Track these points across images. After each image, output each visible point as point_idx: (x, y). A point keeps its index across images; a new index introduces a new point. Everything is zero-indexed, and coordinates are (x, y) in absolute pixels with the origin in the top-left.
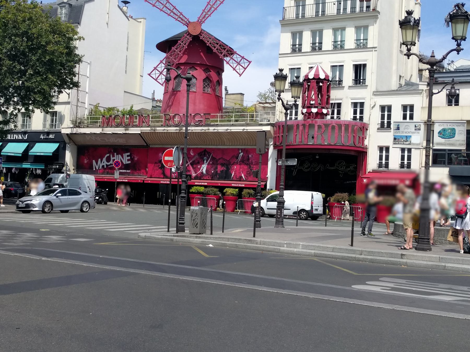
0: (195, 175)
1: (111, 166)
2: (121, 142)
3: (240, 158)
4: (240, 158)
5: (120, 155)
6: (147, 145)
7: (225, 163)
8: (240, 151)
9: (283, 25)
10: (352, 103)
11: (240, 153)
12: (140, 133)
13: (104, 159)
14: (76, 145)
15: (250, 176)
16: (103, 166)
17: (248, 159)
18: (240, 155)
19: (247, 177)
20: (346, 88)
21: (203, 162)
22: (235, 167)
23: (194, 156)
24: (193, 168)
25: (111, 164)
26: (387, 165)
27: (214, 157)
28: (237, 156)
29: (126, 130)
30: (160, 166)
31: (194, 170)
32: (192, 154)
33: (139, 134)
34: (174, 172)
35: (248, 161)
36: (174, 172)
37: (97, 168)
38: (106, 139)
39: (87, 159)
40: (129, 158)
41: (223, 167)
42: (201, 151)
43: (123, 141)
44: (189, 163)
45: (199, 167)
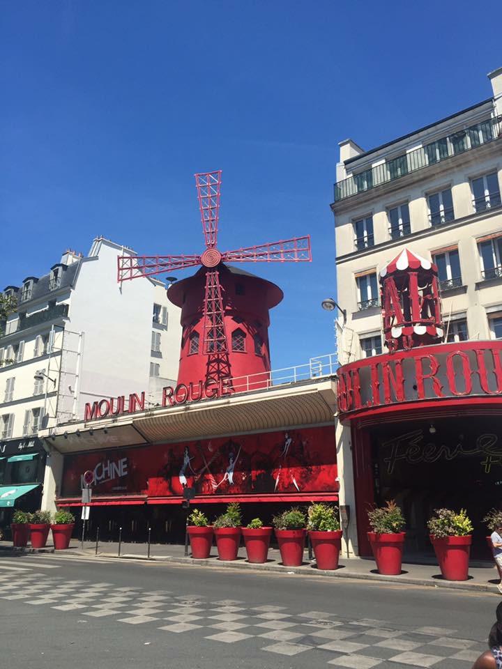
1: (103, 482)
2: (113, 440)
3: (286, 449)
5: (114, 464)
6: (148, 442)
8: (287, 437)
9: (336, 213)
10: (487, 314)
11: (286, 440)
12: (131, 422)
14: (62, 454)
19: (302, 483)
20: (471, 288)
25: (103, 479)
29: (114, 421)
32: (211, 450)
38: (92, 439)
40: (126, 466)
44: (207, 466)
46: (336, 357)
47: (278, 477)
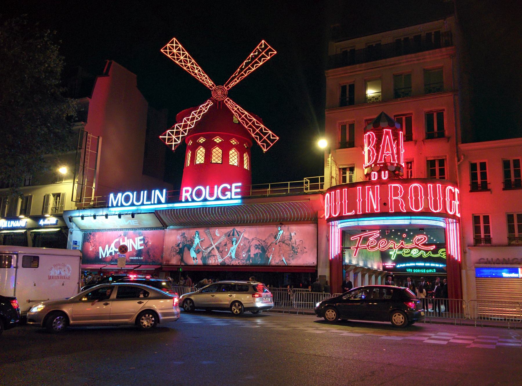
0: (221, 260)
4: (279, 238)
5: (131, 240)
7: (259, 245)
8: (279, 229)
13: (113, 245)
14: (82, 230)
15: (293, 259)
16: (111, 254)
17: (291, 238)
18: (279, 233)
21: (231, 244)
22: (274, 249)
24: (220, 252)
26: (488, 240)
28: (276, 234)
30: (177, 251)
31: (220, 255)
32: (218, 235)
33: (154, 213)
34: (195, 257)
35: (290, 241)
36: (195, 257)
37: (104, 256)
39: (93, 245)
40: (142, 242)
41: (258, 249)
42: (229, 231)
43: (135, 224)
44: (214, 246)
45: (227, 250)
46: (322, 180)
47: (271, 256)
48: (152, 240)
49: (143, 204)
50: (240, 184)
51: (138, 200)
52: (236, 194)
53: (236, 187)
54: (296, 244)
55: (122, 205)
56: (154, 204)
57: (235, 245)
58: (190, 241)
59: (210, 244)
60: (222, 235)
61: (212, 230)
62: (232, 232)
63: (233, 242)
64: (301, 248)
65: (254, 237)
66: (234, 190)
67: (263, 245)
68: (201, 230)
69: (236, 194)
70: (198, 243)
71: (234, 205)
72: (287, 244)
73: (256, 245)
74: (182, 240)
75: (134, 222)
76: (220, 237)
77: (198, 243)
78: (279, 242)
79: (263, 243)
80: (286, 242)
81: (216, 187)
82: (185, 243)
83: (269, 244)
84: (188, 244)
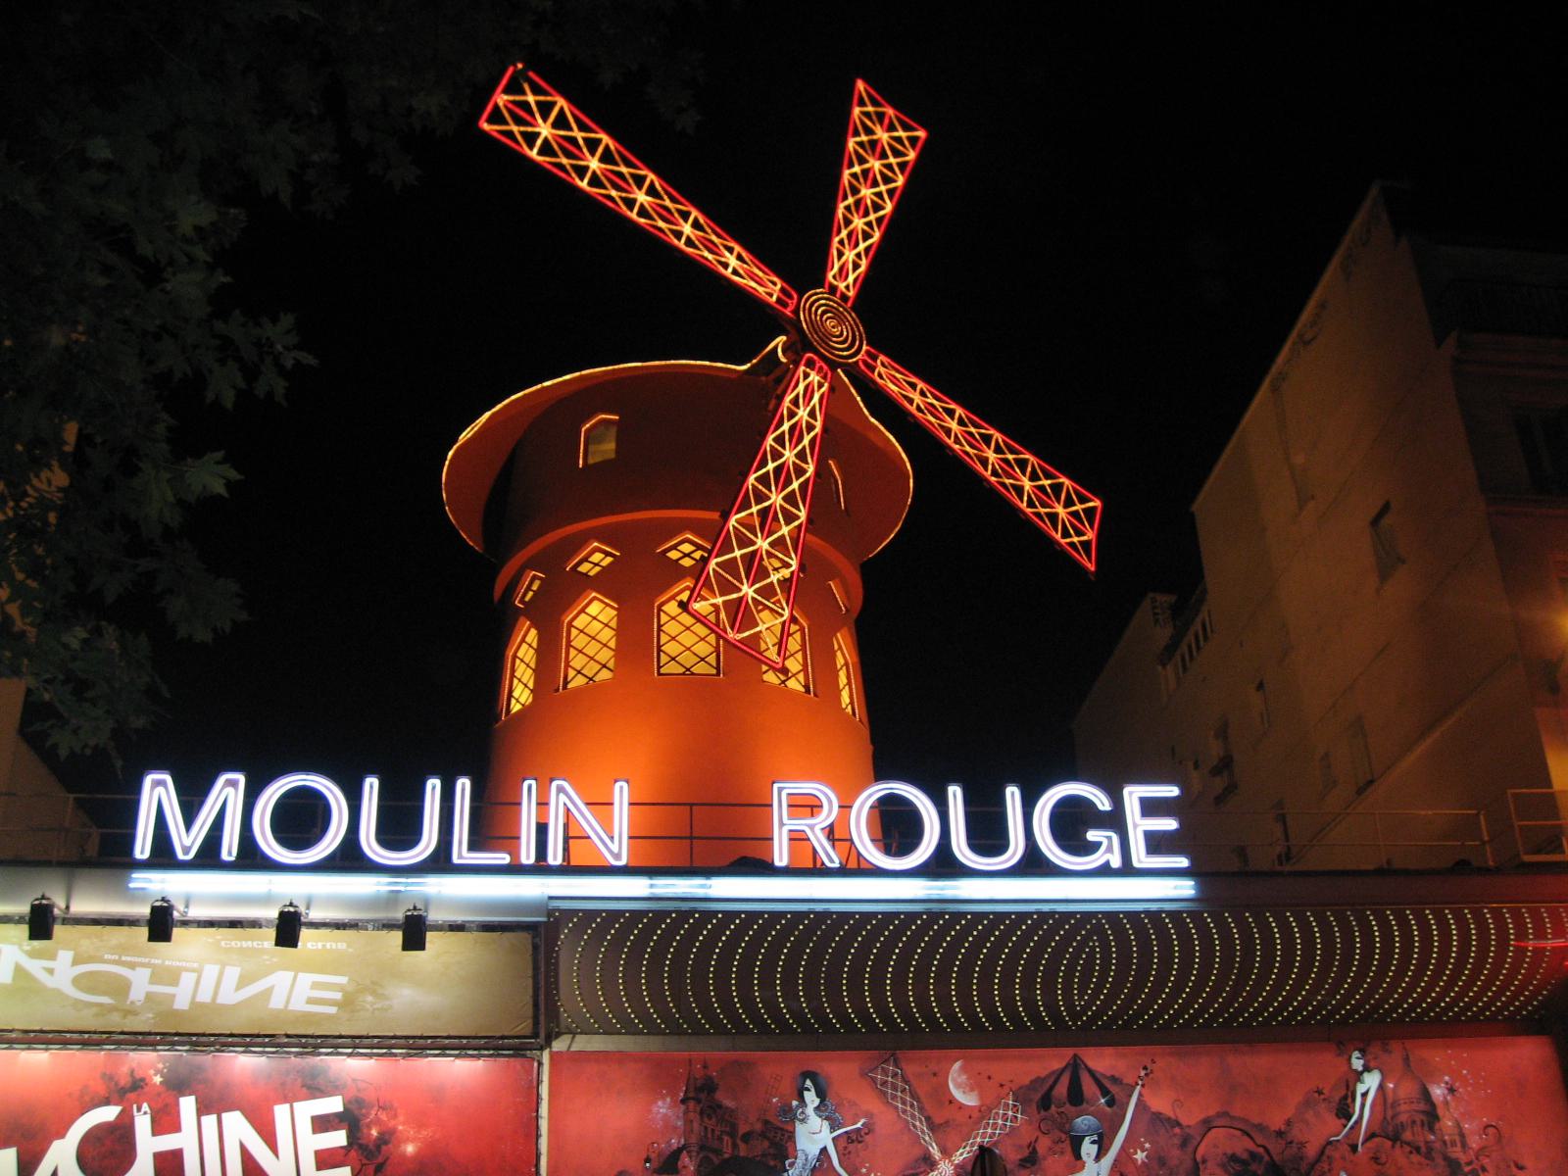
3: (1364, 1111)
4: (1364, 1111)
7: (1253, 1155)
8: (1357, 1064)
11: (1358, 1076)
12: (544, 919)
17: (1431, 1115)
18: (1360, 1089)
21: (1069, 1156)
23: (983, 1113)
27: (1158, 1118)
28: (1343, 1093)
32: (967, 1099)
35: (1431, 1130)
40: (338, 1138)
42: (1043, 1076)
43: (311, 1001)
48: (421, 1126)
49: (440, 862)
50: (1172, 791)
51: (399, 827)
52: (1157, 843)
53: (1150, 807)
54: (1464, 1145)
55: (251, 858)
56: (540, 868)
57: (1098, 1158)
58: (763, 1135)
59: (917, 1152)
60: (999, 1098)
61: (915, 1065)
62: (1065, 1080)
63: (1076, 1143)
64: (1498, 1167)
65: (1211, 1113)
66: (1139, 826)
67: (1276, 1158)
68: (840, 1068)
69: (1157, 843)
70: (824, 1150)
71: (1154, 907)
72: (1418, 1150)
73: (1233, 1158)
74: (696, 1125)
75: (315, 986)
76: (983, 1113)
77: (824, 1150)
78: (1370, 1136)
79: (1275, 1147)
80: (1407, 1135)
81: (1013, 794)
82: (718, 1152)
83: (1311, 1151)
84: (742, 1154)
